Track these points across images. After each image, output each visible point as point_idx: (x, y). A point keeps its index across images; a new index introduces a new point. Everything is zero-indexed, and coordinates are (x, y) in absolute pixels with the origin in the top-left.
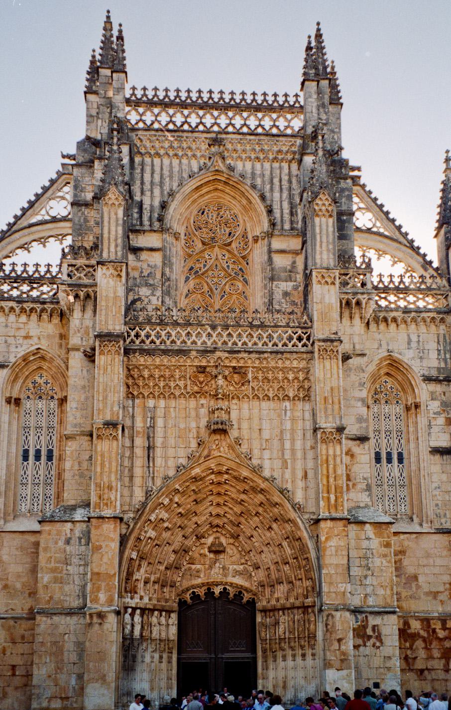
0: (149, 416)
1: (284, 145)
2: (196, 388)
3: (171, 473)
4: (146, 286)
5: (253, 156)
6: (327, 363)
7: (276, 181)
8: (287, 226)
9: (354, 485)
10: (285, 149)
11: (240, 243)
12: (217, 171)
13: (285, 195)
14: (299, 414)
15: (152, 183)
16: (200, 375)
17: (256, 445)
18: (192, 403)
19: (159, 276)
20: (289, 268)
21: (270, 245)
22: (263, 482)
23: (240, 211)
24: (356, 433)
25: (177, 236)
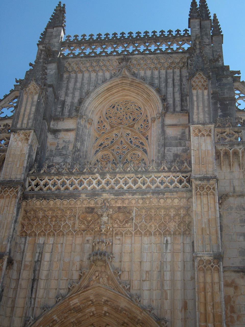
0: (38, 251)
1: (176, 58)
2: (83, 226)
3: (51, 302)
4: (60, 155)
5: (152, 66)
6: (205, 200)
7: (170, 81)
8: (178, 109)
9: (239, 317)
10: (177, 61)
11: (141, 125)
12: (124, 77)
13: (177, 89)
14: (179, 247)
15: (74, 89)
16: (88, 215)
17: (136, 277)
18: (79, 240)
19: (71, 147)
20: (179, 137)
21: (163, 121)
22: (141, 312)
23: (143, 103)
24: (238, 265)
25: (90, 122)
